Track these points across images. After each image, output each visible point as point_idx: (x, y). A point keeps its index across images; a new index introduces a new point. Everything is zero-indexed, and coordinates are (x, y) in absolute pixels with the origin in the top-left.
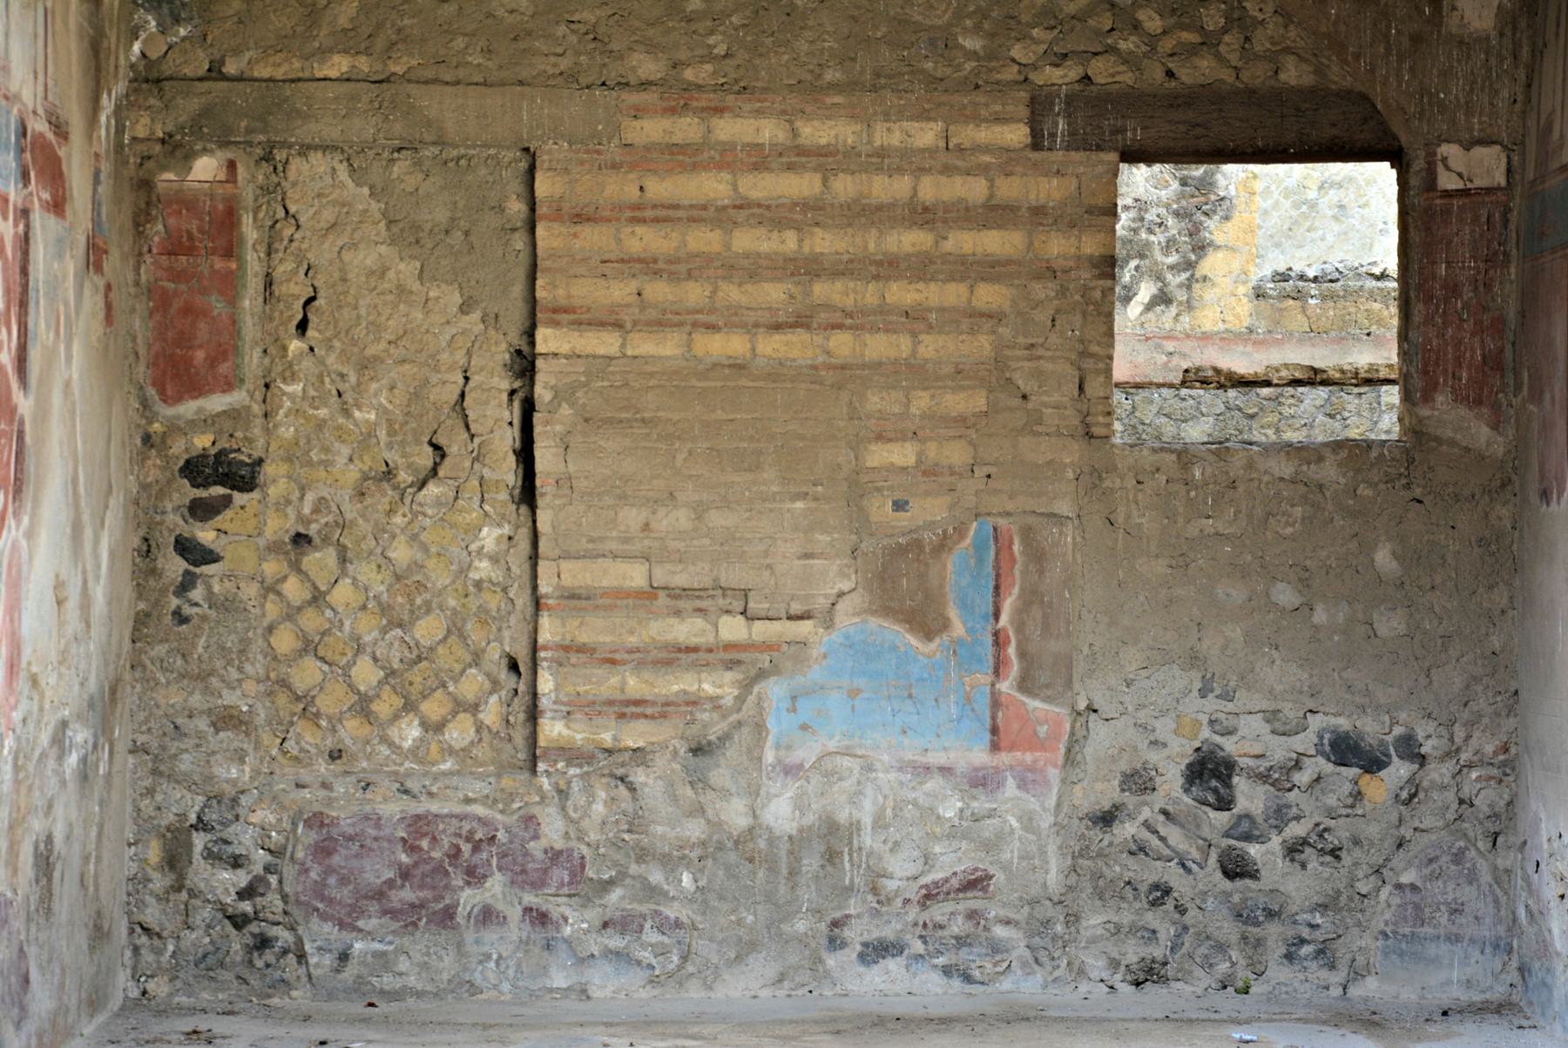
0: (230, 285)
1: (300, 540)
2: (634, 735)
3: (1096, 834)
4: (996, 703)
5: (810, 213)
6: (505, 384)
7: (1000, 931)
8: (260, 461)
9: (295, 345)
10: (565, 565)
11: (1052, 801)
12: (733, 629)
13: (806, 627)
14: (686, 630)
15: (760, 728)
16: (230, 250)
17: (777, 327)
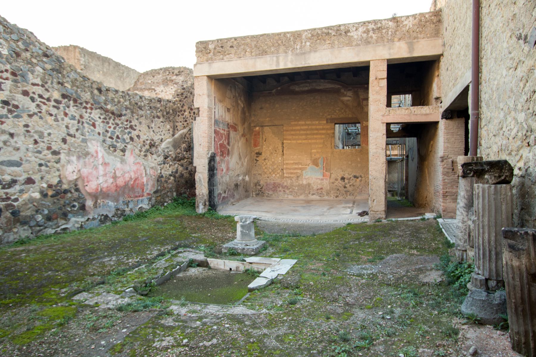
0: (259, 138)
2: (292, 176)
5: (307, 130)
12: (300, 166)
14: (296, 166)
16: (259, 135)
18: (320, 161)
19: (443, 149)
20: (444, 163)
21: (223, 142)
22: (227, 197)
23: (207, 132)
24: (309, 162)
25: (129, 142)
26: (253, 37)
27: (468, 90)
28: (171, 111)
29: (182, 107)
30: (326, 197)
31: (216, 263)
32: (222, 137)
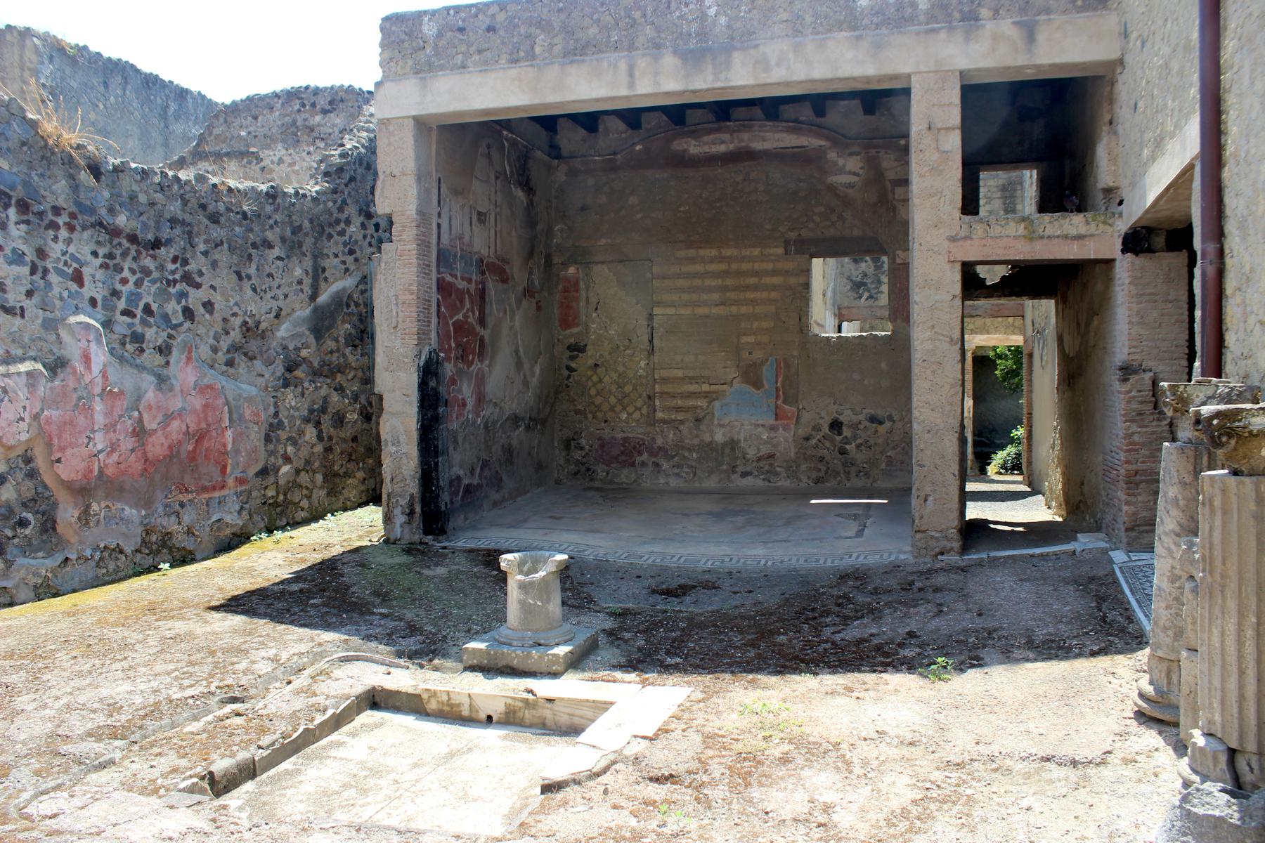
0: (577, 300)
1: (596, 365)
3: (805, 443)
4: (777, 407)
6: (645, 323)
7: (778, 469)
9: (594, 315)
12: (706, 387)
15: (713, 414)
16: (577, 291)
17: (717, 305)
18: (767, 373)
19: (1127, 343)
20: (1128, 386)
21: (465, 316)
22: (480, 486)
23: (414, 288)
24: (732, 373)
25: (181, 325)
27: (1191, 180)
28: (306, 224)
29: (341, 210)
32: (462, 301)
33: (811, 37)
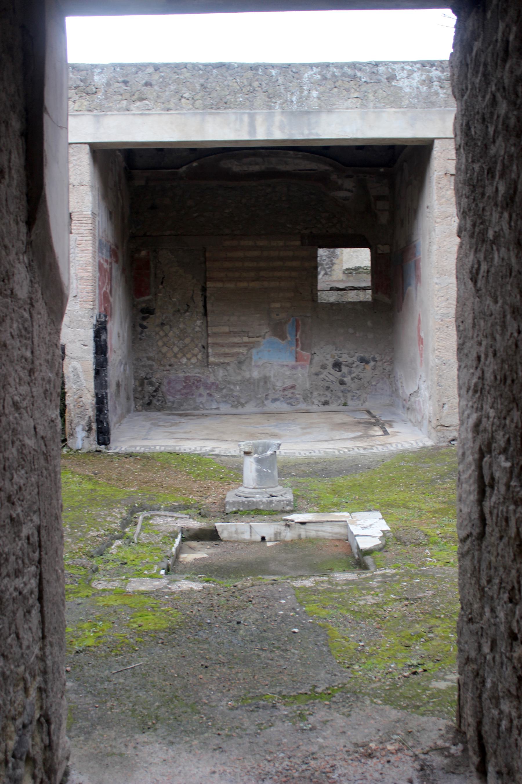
2: (227, 360)
4: (297, 352)
6: (200, 293)
7: (298, 396)
8: (154, 309)
9: (161, 286)
10: (213, 328)
11: (307, 371)
12: (246, 339)
13: (259, 339)
14: (237, 340)
15: (251, 358)
17: (253, 281)
23: (90, 268)
26: (195, 66)
30: (303, 406)
31: (233, 529)
33: (372, 110)
